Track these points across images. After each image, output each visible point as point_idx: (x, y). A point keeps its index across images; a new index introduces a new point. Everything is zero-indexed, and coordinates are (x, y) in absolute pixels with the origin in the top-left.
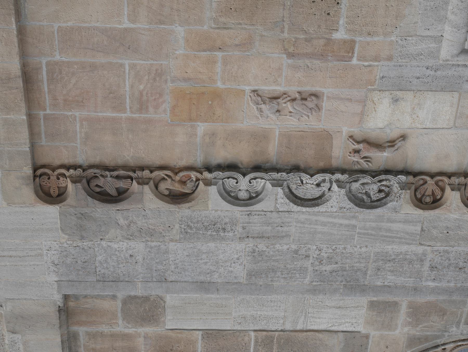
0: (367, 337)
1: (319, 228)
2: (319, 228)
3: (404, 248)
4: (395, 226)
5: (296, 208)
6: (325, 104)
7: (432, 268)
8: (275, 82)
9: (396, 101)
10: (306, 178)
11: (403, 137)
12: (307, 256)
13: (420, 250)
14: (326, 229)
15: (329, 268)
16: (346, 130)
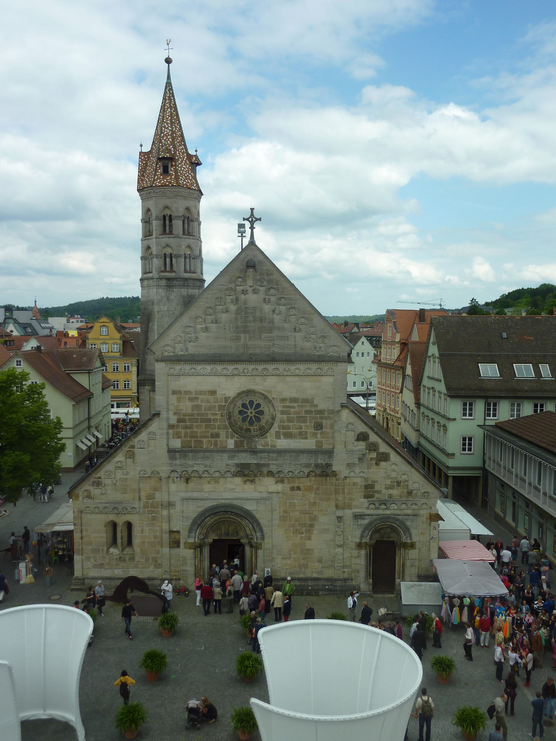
0: (276, 439)
1: (288, 466)
2: (288, 466)
3: (272, 462)
4: (275, 467)
5: (292, 471)
6: (289, 489)
7: (266, 458)
8: (297, 493)
9: (278, 490)
10: (291, 476)
11: (276, 483)
12: (289, 460)
13: (270, 462)
14: (287, 466)
15: (286, 458)
16: (285, 484)
